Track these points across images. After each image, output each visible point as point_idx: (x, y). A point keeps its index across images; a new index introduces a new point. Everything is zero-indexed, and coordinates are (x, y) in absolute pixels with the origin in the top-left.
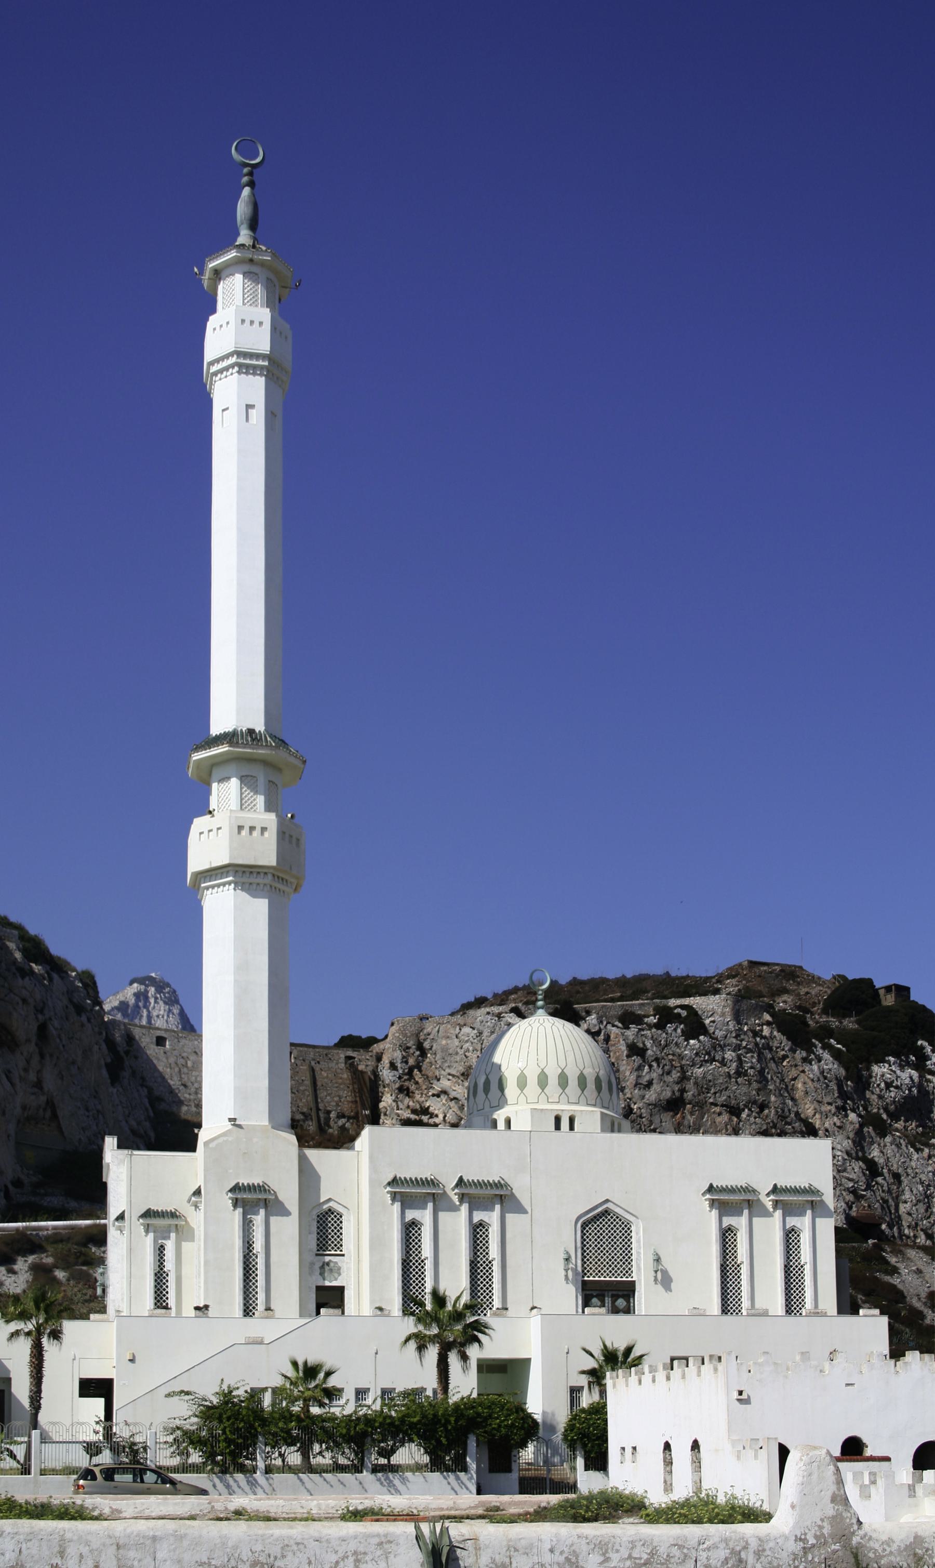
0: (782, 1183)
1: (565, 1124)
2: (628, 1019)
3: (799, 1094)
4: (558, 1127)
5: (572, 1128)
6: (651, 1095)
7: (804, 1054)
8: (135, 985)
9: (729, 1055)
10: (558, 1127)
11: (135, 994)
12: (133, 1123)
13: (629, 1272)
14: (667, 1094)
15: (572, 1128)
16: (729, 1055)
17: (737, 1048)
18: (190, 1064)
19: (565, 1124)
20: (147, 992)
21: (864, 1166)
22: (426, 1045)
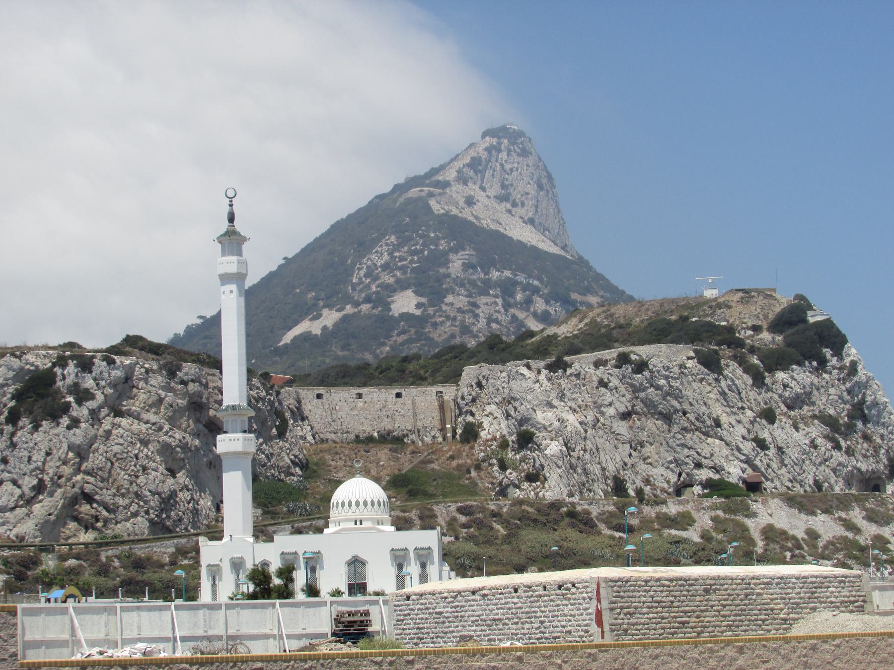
0: (419, 546)
1: (358, 523)
2: (598, 364)
3: (710, 402)
4: (356, 524)
5: (361, 524)
6: (611, 411)
7: (716, 375)
8: (487, 138)
9: (662, 382)
10: (356, 524)
11: (486, 149)
12: (292, 457)
13: (364, 578)
14: (622, 409)
15: (361, 524)
16: (662, 382)
17: (666, 378)
18: (337, 408)
19: (358, 523)
20: (500, 144)
21: (755, 445)
22: (484, 382)
